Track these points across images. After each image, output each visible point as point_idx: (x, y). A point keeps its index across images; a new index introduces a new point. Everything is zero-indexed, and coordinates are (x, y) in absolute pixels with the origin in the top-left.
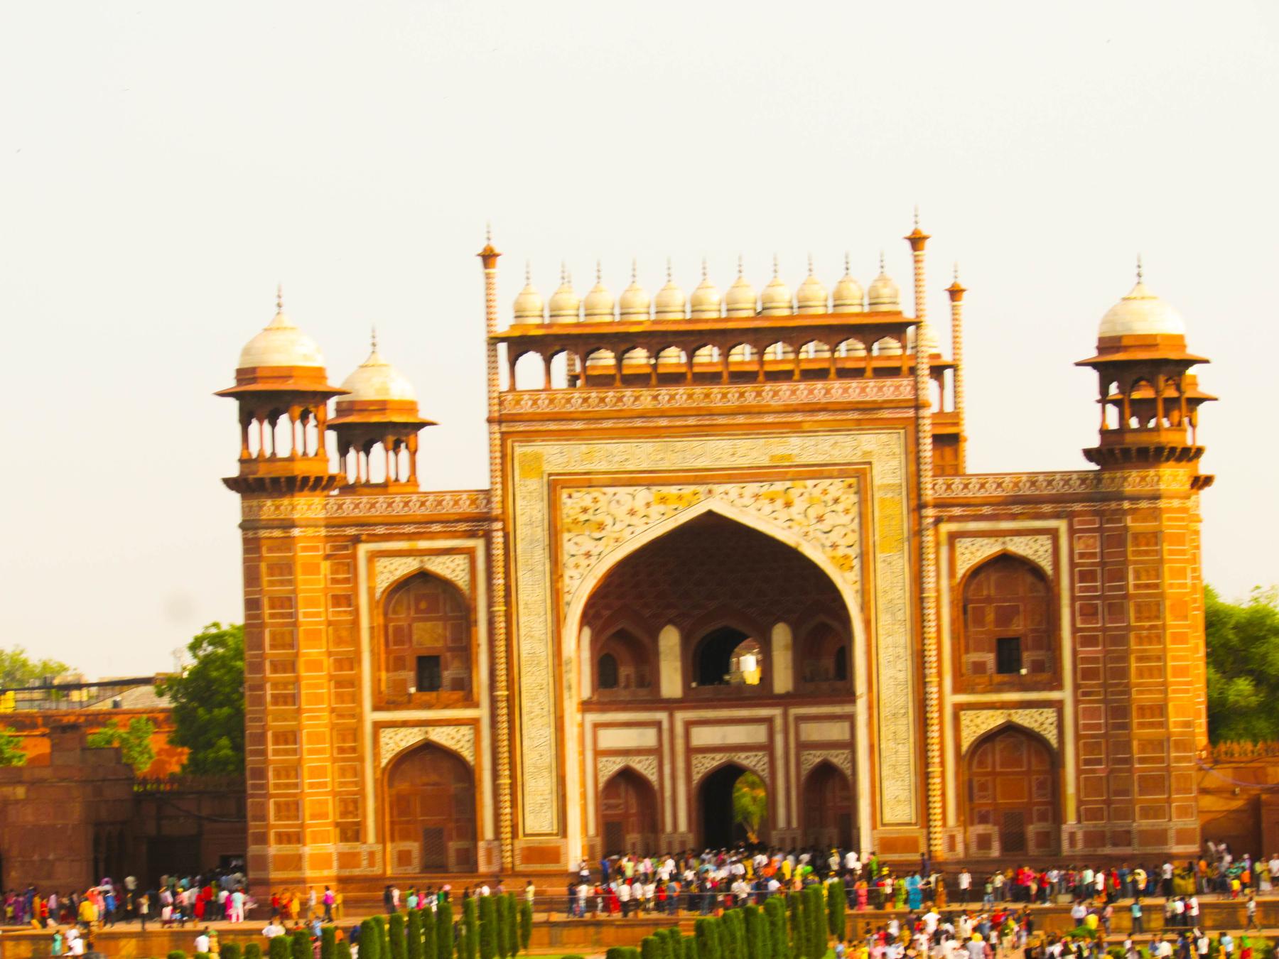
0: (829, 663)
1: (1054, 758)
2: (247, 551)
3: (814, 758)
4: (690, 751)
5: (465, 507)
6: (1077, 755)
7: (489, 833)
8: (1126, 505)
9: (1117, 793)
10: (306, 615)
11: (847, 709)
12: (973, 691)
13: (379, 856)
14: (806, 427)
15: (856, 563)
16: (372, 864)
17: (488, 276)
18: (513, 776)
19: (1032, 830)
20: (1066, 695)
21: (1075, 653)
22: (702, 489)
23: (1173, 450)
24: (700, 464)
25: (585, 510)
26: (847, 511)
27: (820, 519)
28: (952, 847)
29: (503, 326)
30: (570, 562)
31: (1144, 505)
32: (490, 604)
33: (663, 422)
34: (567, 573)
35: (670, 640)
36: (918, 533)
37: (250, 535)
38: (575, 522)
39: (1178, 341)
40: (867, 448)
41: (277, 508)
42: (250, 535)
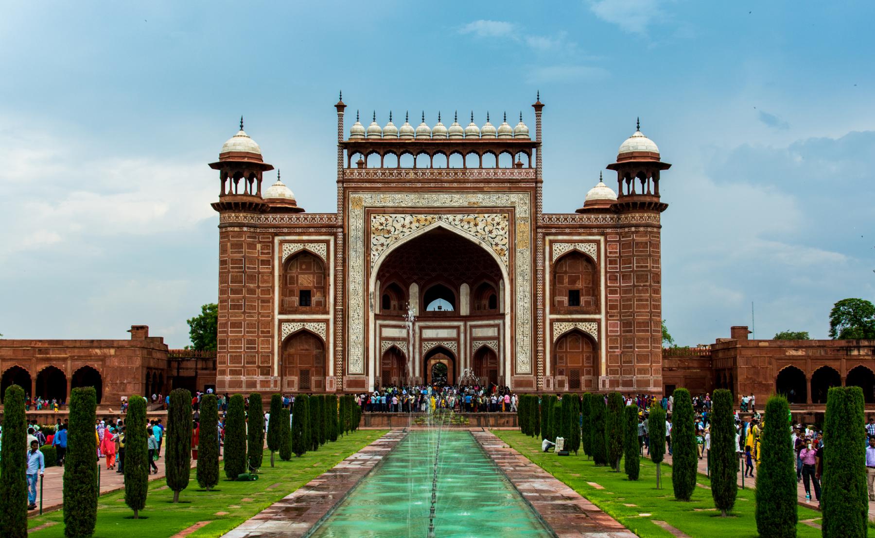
0: (486, 302)
1: (595, 346)
2: (221, 238)
3: (479, 344)
4: (422, 340)
5: (325, 221)
6: (607, 344)
7: (331, 373)
8: (633, 229)
9: (624, 362)
10: (248, 268)
11: (497, 322)
12: (559, 313)
13: (279, 383)
14: (485, 189)
15: (507, 253)
16: (275, 386)
17: (341, 117)
18: (344, 347)
19: (583, 379)
20: (602, 316)
21: (606, 297)
22: (436, 216)
23: (656, 204)
24: (435, 205)
25: (381, 224)
26: (503, 229)
27: (491, 232)
28: (548, 386)
29: (346, 139)
30: (374, 248)
31: (642, 229)
32: (335, 267)
33: (419, 185)
34: (373, 253)
35: (414, 289)
36: (535, 240)
37: (224, 230)
38: (377, 229)
39: (656, 156)
40: (513, 200)
41: (237, 217)
42: (224, 230)
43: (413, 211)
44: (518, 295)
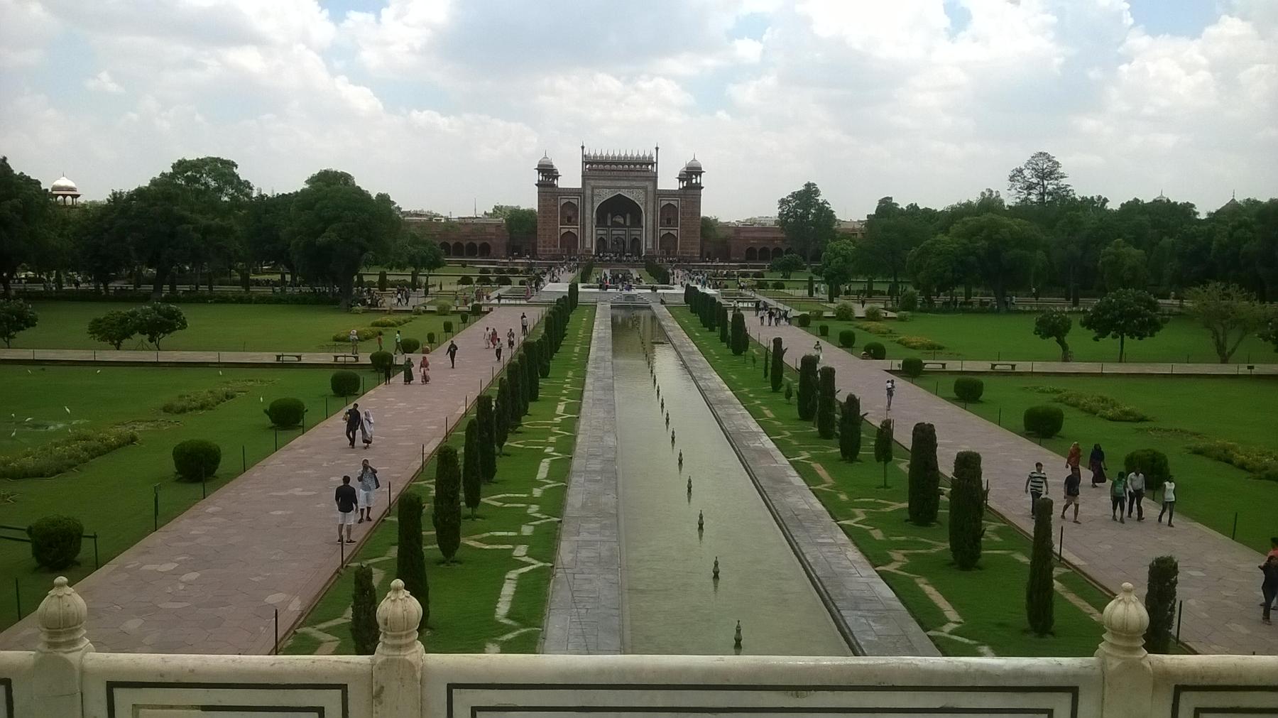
43: (609, 188)
44: (648, 219)
